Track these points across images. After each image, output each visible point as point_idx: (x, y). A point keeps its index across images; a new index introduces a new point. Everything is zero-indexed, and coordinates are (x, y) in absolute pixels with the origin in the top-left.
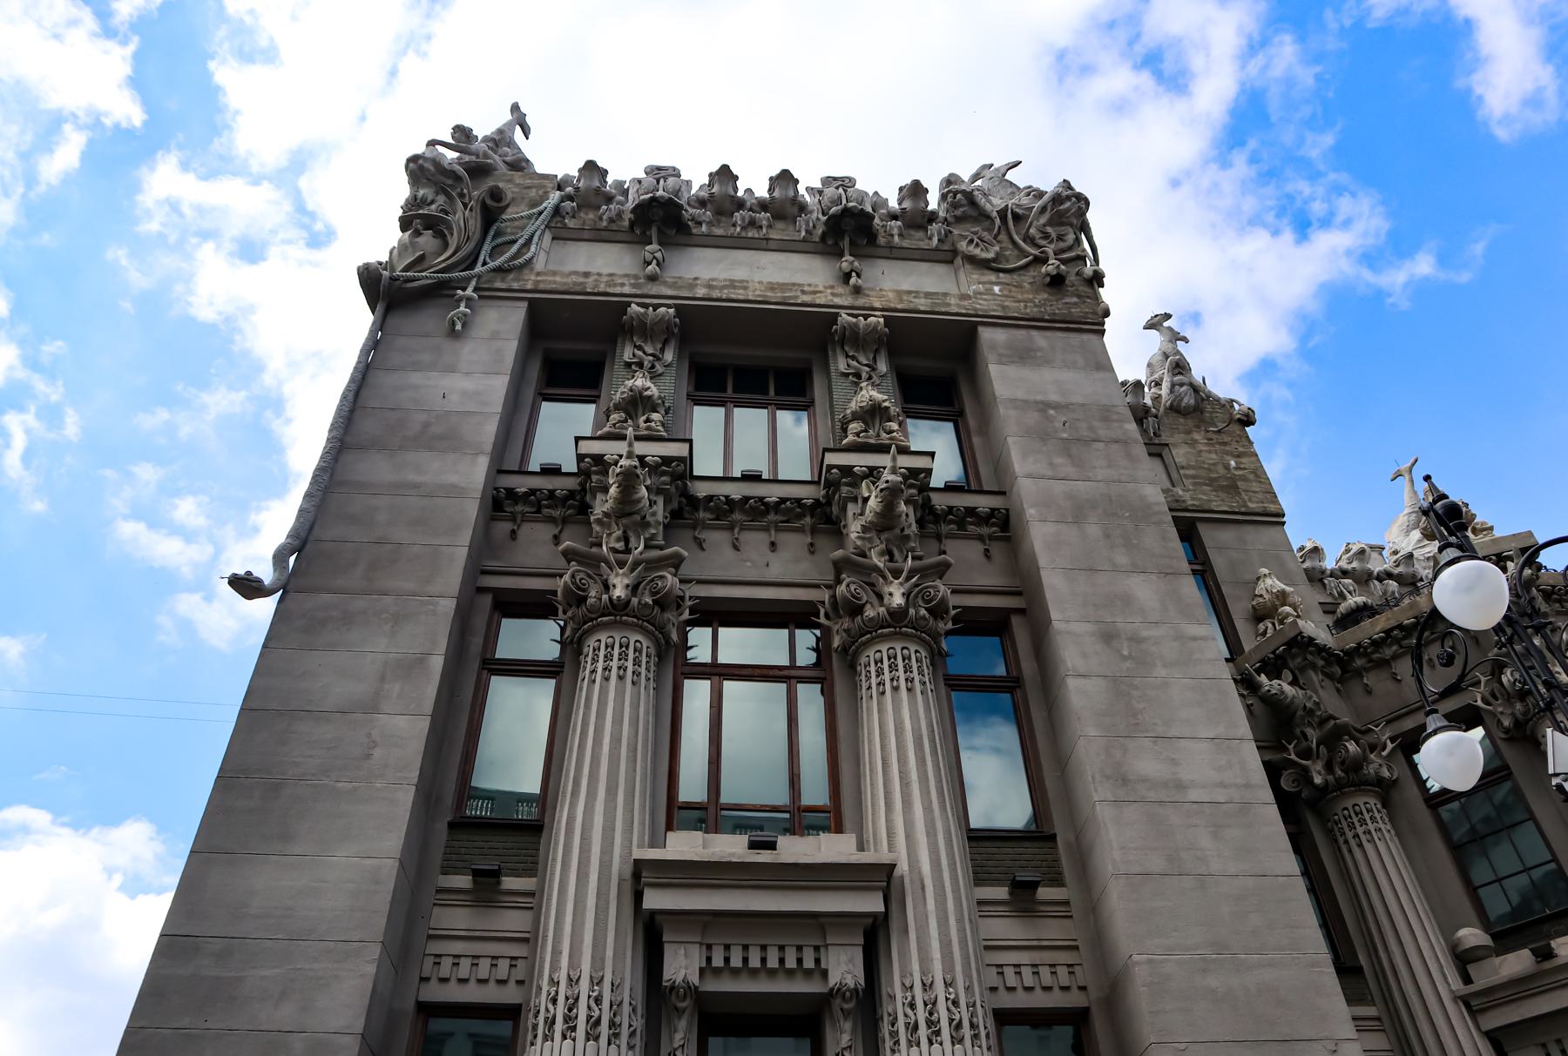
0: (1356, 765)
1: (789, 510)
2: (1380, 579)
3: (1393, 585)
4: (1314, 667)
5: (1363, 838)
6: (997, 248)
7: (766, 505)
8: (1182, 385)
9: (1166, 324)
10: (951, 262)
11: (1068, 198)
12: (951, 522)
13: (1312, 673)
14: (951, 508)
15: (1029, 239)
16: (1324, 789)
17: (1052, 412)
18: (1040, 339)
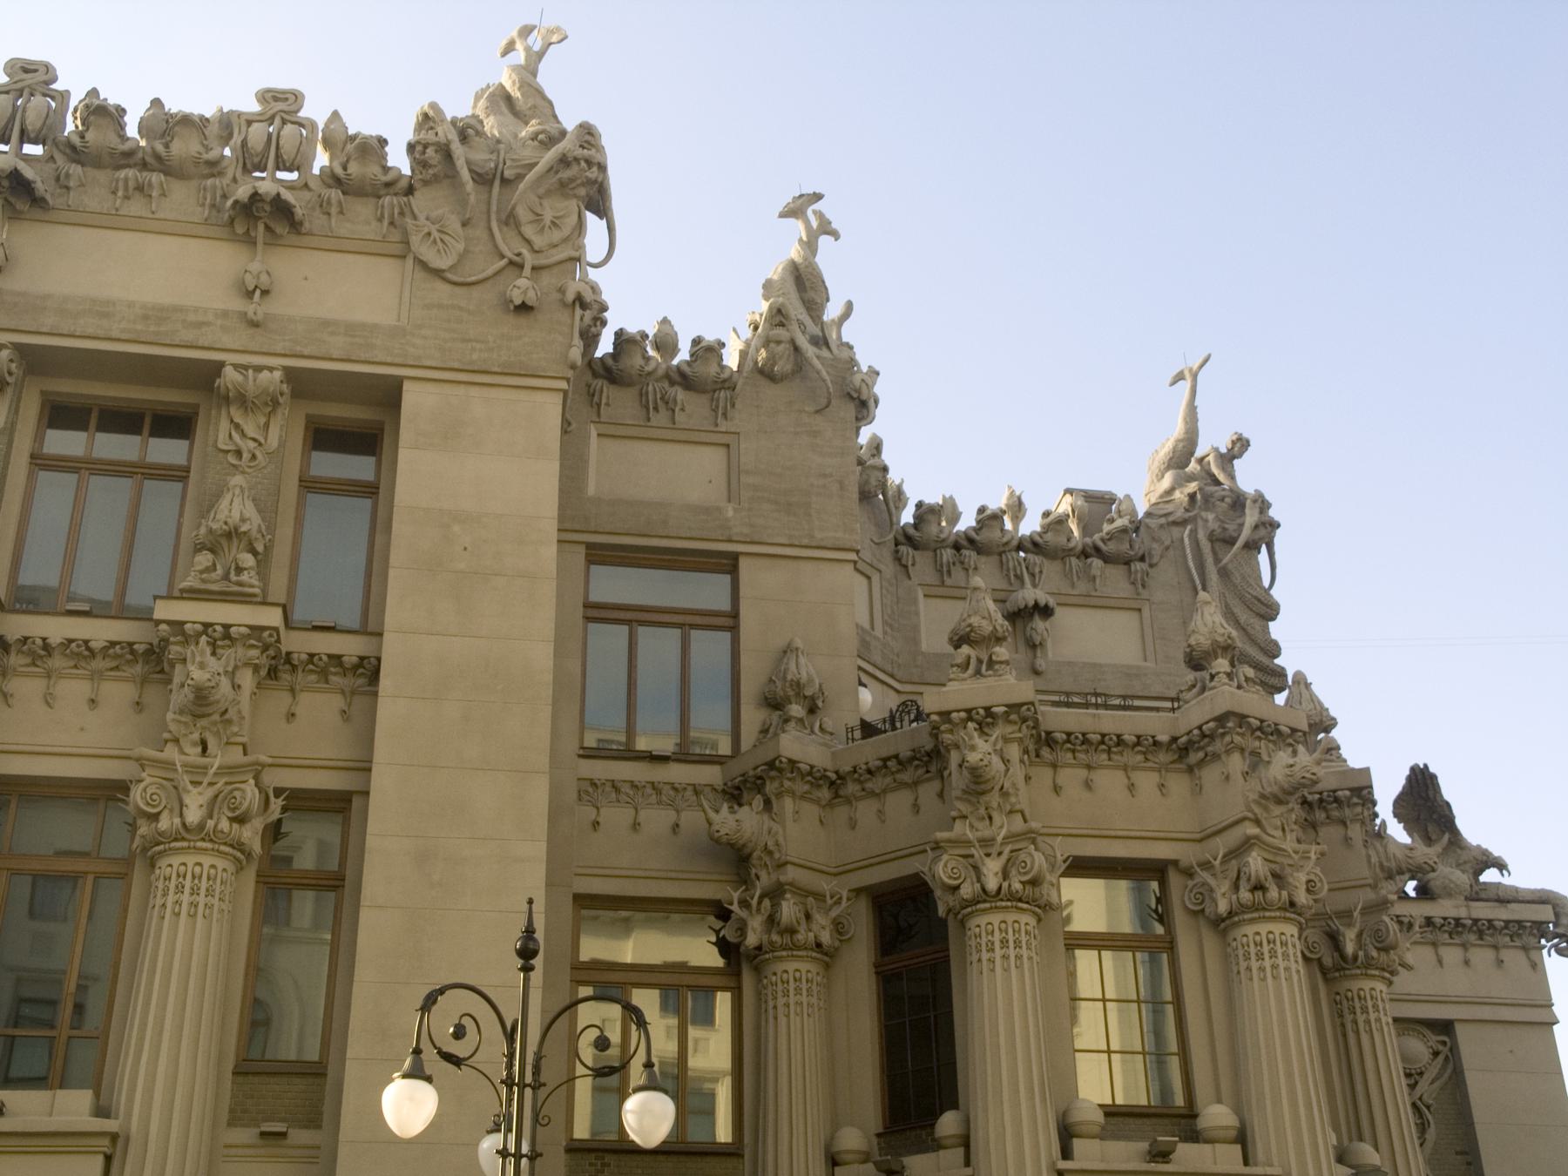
0: (792, 931)
1: (117, 656)
2: (1084, 554)
3: (1097, 563)
4: (793, 793)
5: (781, 1010)
6: (461, 247)
7: (88, 649)
8: (779, 342)
9: (817, 206)
10: (404, 257)
11: (576, 160)
12: (312, 671)
13: (788, 803)
14: (312, 656)
15: (510, 220)
16: (759, 948)
17: (456, 528)
18: (481, 404)
